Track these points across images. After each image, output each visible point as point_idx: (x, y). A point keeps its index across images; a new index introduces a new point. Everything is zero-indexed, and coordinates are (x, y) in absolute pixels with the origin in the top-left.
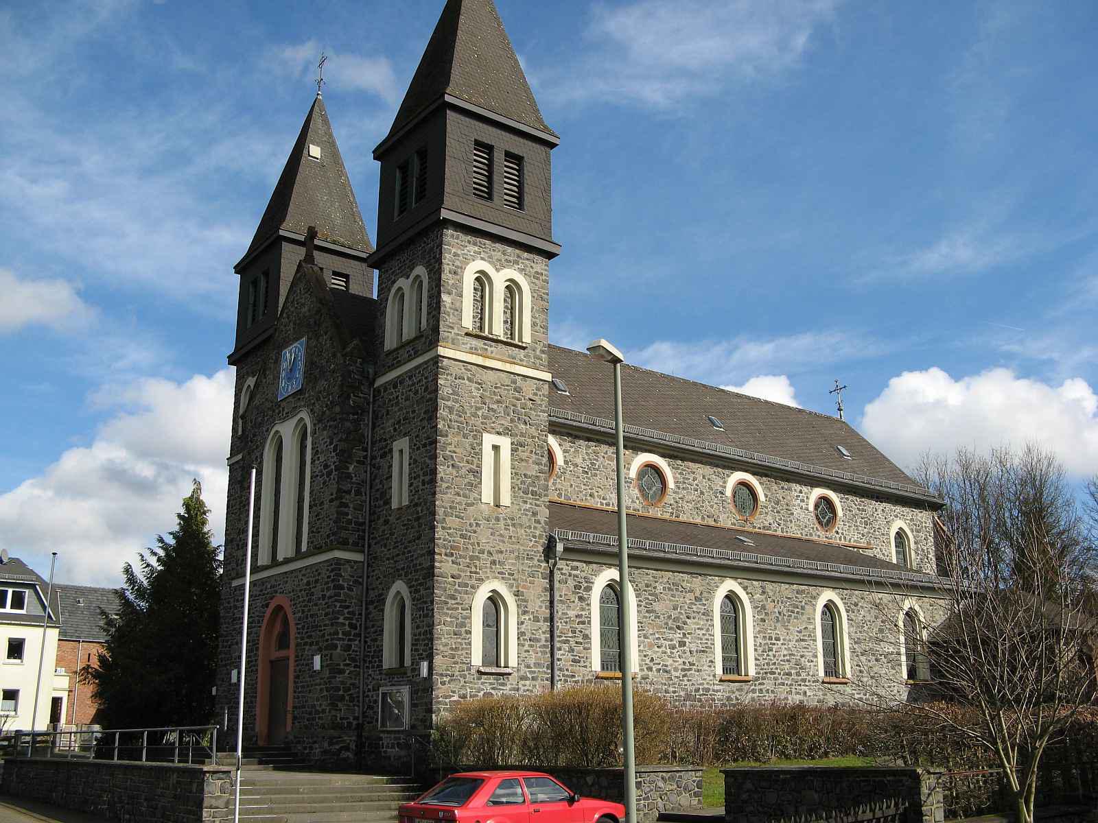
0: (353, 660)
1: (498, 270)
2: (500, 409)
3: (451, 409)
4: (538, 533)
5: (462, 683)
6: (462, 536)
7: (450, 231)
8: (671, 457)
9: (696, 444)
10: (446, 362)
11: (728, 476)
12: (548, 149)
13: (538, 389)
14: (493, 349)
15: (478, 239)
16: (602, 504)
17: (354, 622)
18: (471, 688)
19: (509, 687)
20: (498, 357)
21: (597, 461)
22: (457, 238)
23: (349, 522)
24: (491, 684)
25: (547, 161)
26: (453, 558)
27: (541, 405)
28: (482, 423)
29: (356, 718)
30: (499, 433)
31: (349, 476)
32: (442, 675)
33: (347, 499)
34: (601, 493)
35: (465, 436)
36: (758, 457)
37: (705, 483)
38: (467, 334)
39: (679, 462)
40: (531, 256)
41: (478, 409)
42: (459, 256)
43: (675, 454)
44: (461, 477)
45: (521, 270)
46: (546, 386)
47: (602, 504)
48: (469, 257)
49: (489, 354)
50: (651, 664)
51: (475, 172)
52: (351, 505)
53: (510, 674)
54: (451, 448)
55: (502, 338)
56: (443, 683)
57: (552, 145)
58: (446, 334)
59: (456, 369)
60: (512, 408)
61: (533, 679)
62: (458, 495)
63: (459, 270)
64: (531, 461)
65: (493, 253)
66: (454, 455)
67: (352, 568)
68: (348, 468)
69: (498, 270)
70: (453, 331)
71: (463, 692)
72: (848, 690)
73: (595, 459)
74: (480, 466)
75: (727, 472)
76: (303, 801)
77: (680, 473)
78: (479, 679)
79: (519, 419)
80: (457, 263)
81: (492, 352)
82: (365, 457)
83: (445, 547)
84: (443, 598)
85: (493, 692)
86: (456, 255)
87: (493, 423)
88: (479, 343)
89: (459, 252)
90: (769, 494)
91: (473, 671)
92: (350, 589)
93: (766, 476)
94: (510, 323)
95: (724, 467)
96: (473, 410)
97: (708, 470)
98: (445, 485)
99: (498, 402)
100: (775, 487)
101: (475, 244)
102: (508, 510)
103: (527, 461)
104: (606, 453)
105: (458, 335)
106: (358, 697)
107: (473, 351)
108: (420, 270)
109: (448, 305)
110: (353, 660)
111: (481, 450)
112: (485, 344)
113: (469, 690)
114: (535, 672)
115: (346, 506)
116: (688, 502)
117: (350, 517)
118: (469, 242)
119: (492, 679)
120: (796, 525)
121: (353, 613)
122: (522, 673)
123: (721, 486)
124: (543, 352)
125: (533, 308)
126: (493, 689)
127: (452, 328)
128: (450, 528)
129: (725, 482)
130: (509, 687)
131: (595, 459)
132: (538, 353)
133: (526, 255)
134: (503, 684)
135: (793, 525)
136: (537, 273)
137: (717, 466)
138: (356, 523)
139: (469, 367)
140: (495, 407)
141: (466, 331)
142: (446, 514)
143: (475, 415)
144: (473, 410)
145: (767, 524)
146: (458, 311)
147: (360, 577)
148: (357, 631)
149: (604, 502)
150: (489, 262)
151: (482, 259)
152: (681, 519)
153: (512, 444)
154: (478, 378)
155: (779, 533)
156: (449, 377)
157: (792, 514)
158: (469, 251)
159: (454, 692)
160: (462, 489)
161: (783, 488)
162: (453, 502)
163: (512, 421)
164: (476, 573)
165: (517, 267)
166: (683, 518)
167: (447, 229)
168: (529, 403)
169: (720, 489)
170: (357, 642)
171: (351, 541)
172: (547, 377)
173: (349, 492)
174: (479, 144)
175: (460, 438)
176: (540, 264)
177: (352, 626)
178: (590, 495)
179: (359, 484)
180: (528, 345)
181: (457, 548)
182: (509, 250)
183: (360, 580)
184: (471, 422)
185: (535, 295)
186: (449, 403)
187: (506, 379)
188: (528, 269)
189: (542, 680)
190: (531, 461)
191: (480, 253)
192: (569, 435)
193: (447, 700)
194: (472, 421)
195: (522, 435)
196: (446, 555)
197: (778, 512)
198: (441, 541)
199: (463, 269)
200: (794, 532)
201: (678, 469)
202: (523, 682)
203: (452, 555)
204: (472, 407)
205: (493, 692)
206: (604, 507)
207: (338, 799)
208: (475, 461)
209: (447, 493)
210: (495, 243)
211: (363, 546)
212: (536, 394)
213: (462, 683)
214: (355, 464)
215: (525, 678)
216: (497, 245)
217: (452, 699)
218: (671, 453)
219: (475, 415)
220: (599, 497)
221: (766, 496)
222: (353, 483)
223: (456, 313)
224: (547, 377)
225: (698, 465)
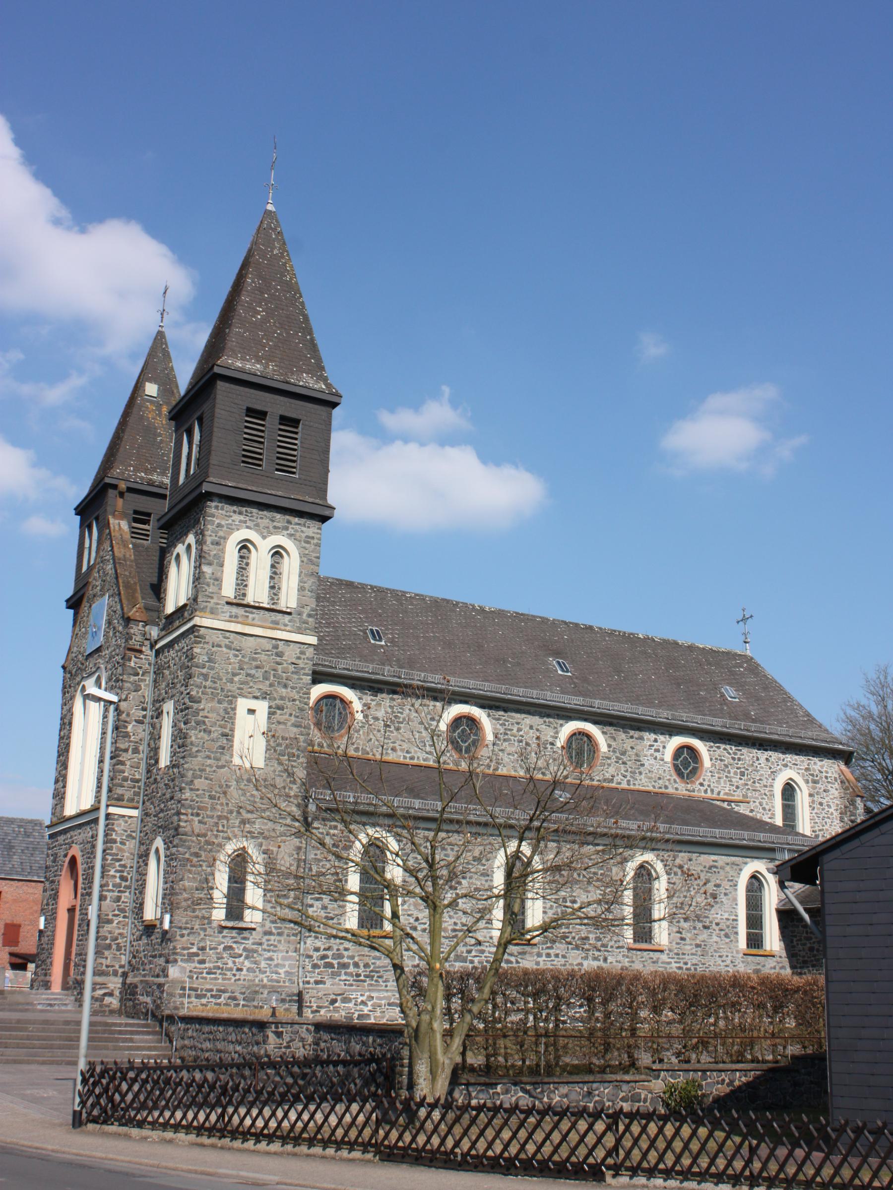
0: (123, 911)
1: (264, 538)
2: (259, 674)
3: (205, 677)
4: (292, 793)
5: (202, 936)
6: (211, 797)
7: (213, 504)
8: (490, 707)
9: (519, 693)
10: (202, 631)
11: (562, 725)
12: (329, 409)
13: (302, 653)
14: (257, 615)
15: (244, 509)
16: (405, 757)
17: (125, 874)
18: (211, 941)
19: (251, 941)
20: (259, 623)
21: (402, 713)
22: (222, 509)
23: (125, 779)
24: (232, 938)
25: (330, 416)
26: (200, 818)
27: (303, 668)
28: (239, 689)
29: (122, 966)
30: (256, 698)
31: (127, 735)
32: (180, 928)
33: (124, 757)
34: (405, 746)
35: (220, 702)
36: (599, 705)
37: (532, 733)
38: (228, 603)
39: (502, 713)
40: (302, 521)
41: (234, 675)
42: (223, 526)
43: (497, 704)
44: (213, 740)
45: (290, 536)
46: (311, 650)
47: (405, 757)
48: (234, 527)
49: (250, 621)
50: (416, 924)
51: (245, 439)
52: (128, 763)
53: (254, 929)
54: (205, 713)
55: (265, 605)
56: (182, 936)
57: (334, 405)
58: (205, 604)
59: (217, 638)
60: (272, 672)
61: (279, 934)
62: (209, 757)
63: (222, 541)
64: (289, 723)
65: (259, 521)
66: (206, 720)
67: (126, 822)
68: (127, 727)
69: (264, 538)
70: (212, 601)
71: (202, 944)
72: (664, 957)
73: (399, 712)
74: (232, 730)
75: (561, 722)
76: (28, 1038)
77: (501, 725)
78: (220, 932)
79: (279, 683)
80: (221, 534)
81: (254, 619)
82: (144, 717)
83: (190, 807)
84: (187, 856)
85: (234, 946)
86: (219, 525)
87: (251, 687)
88: (240, 611)
89: (223, 523)
90: (613, 744)
91: (215, 924)
92: (123, 843)
93: (611, 724)
94: (274, 588)
95: (559, 717)
96: (230, 676)
97: (536, 720)
98: (195, 749)
99: (257, 667)
100: (623, 736)
101: (240, 513)
102: (262, 771)
103: (285, 724)
104: (413, 705)
105: (217, 604)
106: (125, 946)
107: (233, 618)
108: (191, 539)
109: (207, 576)
110: (123, 911)
111: (235, 714)
112: (246, 612)
113: (208, 943)
114: (280, 928)
115: (122, 763)
116: (509, 754)
117: (126, 774)
118: (235, 512)
119: (234, 933)
120: (646, 777)
121: (124, 866)
122: (267, 928)
123: (552, 737)
124: (309, 616)
125: (301, 573)
126: (235, 942)
127: (212, 598)
128: (198, 790)
129: (557, 733)
130: (251, 941)
131: (399, 712)
132: (304, 616)
133: (296, 520)
134: (245, 938)
135: (643, 776)
136: (307, 537)
137: (549, 716)
138: (133, 780)
139: (228, 634)
140: (253, 672)
141: (226, 599)
142: (195, 777)
143: (231, 681)
144: (230, 676)
145: (608, 776)
146: (218, 580)
147: (134, 832)
148: (128, 883)
149: (408, 755)
150: (256, 531)
151: (248, 527)
152: (499, 772)
153: (270, 707)
154: (236, 645)
155: (624, 785)
156: (206, 646)
157: (643, 765)
158: (233, 521)
159: (193, 944)
160: (212, 752)
161: (632, 737)
162: (203, 765)
163: (271, 685)
164: (223, 831)
165: (285, 532)
166: (503, 771)
167: (211, 501)
168: (291, 668)
169: (551, 740)
170: (127, 894)
171: (126, 797)
172: (313, 640)
173: (126, 750)
174: (250, 412)
175: (215, 704)
176: (311, 528)
177: (123, 878)
178: (392, 749)
179: (137, 742)
180: (292, 611)
181: (205, 809)
182: (278, 516)
183: (134, 834)
184: (226, 689)
185: (305, 560)
186: (204, 671)
187: (268, 645)
188: (298, 534)
189: (288, 935)
190: (289, 723)
191: (245, 522)
192: (371, 689)
193: (185, 952)
194: (229, 686)
195: (282, 698)
196: (192, 815)
197: (624, 763)
198: (188, 802)
199: (225, 539)
200: (643, 783)
201: (499, 719)
202: (267, 937)
203: (198, 815)
204: (228, 673)
205: (234, 946)
206: (408, 761)
207: (61, 1038)
208: (229, 725)
209: (196, 757)
210: (263, 510)
211: (138, 802)
212: (299, 658)
213: (202, 936)
214: (134, 723)
215: (270, 933)
216: (265, 513)
217: (191, 951)
218: (490, 704)
219: (231, 681)
220: (402, 750)
221: (609, 746)
222: (131, 742)
223: (216, 583)
224: (313, 640)
225: (523, 716)
